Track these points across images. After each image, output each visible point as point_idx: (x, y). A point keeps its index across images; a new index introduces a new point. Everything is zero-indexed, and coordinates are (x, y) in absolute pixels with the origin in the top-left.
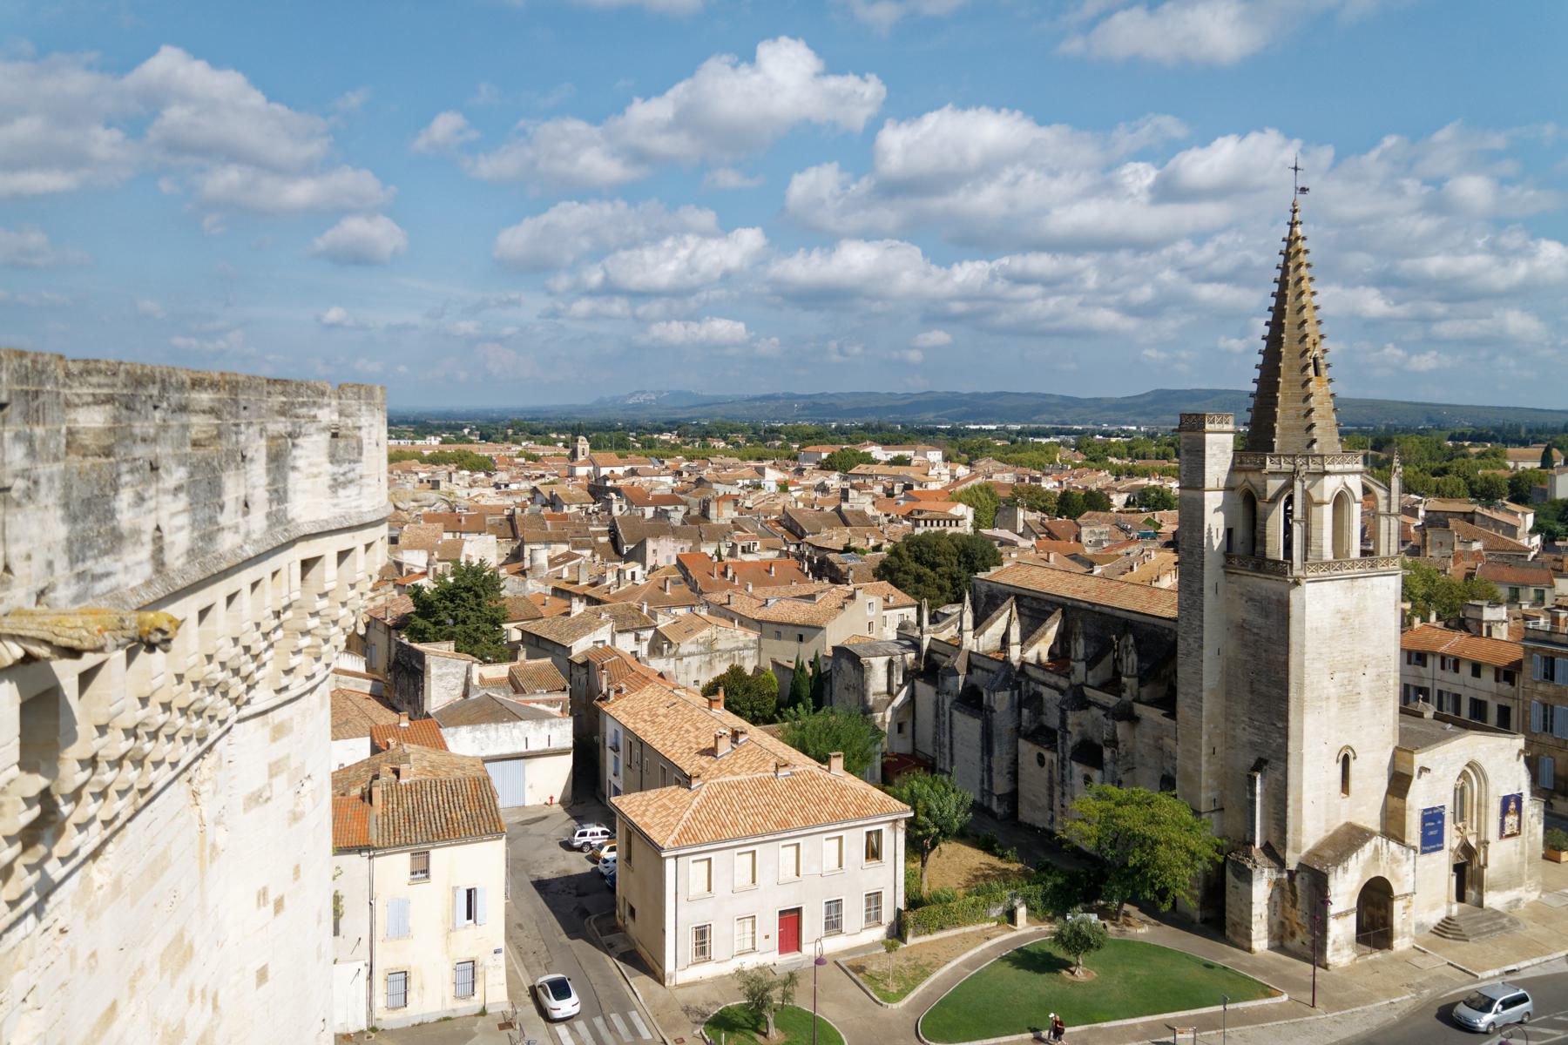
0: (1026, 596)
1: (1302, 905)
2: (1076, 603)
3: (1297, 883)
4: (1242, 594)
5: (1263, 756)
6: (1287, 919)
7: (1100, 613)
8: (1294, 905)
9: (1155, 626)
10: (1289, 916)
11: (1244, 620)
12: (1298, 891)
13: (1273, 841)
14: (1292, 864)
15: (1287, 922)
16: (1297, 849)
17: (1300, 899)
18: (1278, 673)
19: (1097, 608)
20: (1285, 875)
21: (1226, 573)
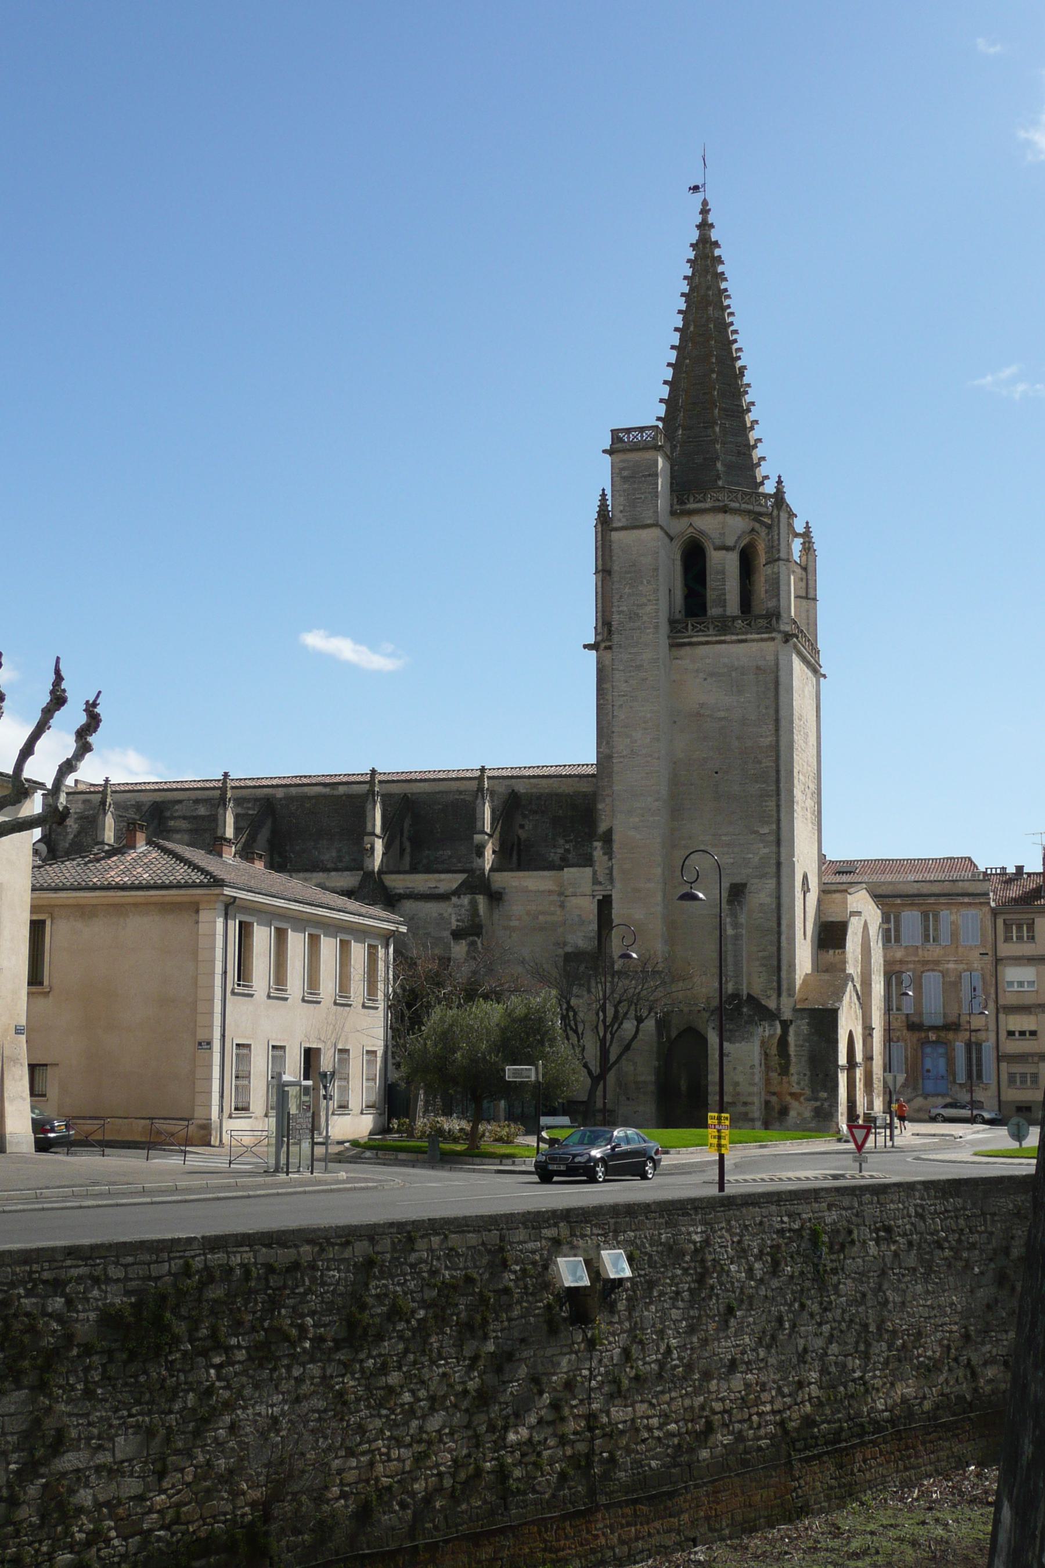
0: (180, 802)
1: (797, 1066)
2: (293, 791)
3: (791, 1039)
4: (697, 671)
5: (737, 880)
6: (774, 1094)
7: (349, 796)
8: (784, 1070)
9: (460, 793)
10: (776, 1089)
11: (702, 705)
12: (792, 1050)
13: (756, 992)
14: (787, 1015)
15: (774, 1099)
16: (791, 993)
17: (793, 1059)
18: (760, 763)
19: (342, 790)
20: (779, 1031)
21: (672, 646)
